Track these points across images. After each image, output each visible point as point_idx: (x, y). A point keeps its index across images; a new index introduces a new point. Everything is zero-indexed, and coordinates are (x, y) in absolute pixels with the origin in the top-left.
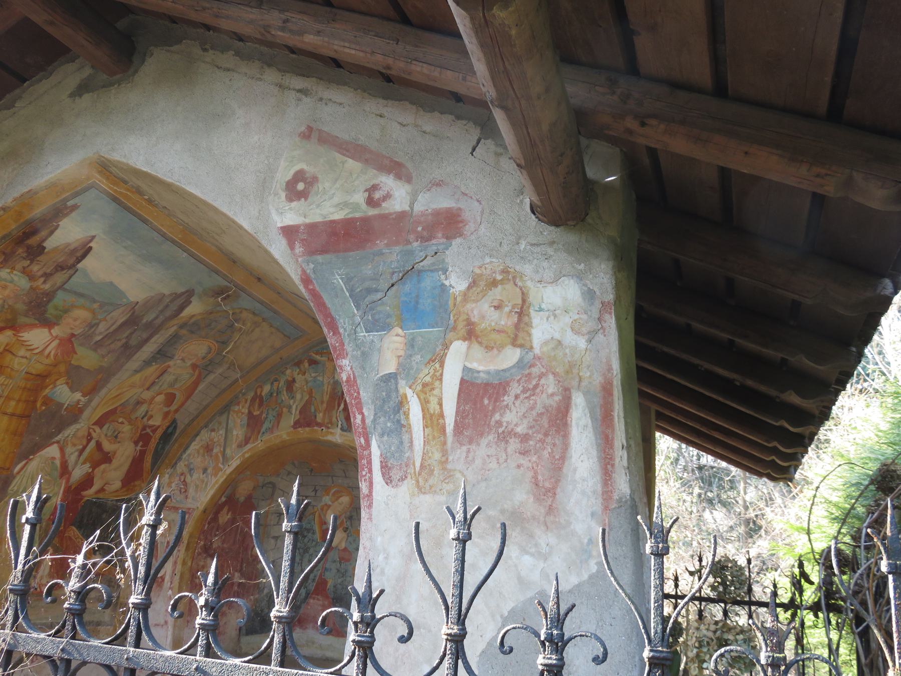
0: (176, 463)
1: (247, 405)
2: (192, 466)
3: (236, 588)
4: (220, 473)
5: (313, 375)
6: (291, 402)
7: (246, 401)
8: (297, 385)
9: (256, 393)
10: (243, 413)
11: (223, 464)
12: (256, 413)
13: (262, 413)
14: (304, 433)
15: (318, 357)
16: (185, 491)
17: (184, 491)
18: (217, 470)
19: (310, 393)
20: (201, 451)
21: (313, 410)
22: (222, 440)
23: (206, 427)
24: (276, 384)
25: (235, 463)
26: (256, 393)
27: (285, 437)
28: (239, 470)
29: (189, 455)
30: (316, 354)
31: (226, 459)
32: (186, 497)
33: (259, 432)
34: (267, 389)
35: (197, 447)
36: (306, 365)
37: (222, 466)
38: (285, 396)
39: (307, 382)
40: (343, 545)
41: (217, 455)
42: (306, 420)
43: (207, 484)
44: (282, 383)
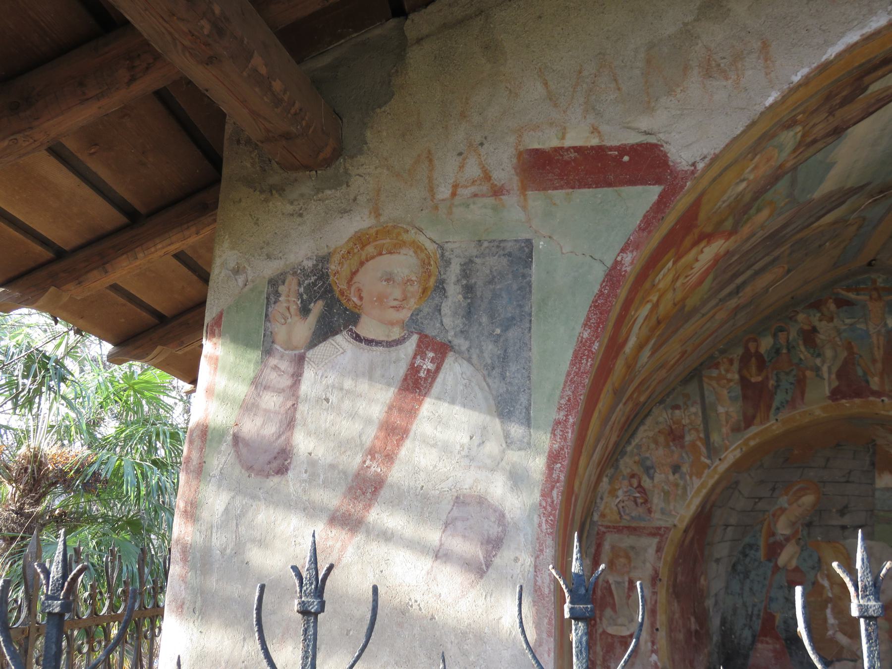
0: (617, 460)
1: (736, 366)
2: (648, 463)
3: (694, 640)
4: (706, 471)
5: (847, 321)
6: (818, 361)
7: (731, 362)
8: (822, 337)
9: (747, 349)
10: (729, 381)
11: (709, 457)
12: (756, 379)
13: (767, 378)
14: (851, 406)
15: (852, 296)
16: (646, 501)
17: (643, 498)
18: (698, 469)
19: (849, 347)
20: (661, 439)
21: (860, 373)
22: (699, 421)
23: (661, 402)
24: (782, 336)
25: (731, 456)
26: (747, 349)
27: (818, 413)
28: (737, 466)
29: (639, 446)
30: (849, 289)
31: (713, 451)
32: (650, 511)
33: (769, 407)
34: (766, 344)
35: (651, 434)
36: (832, 306)
37: (708, 461)
38: (803, 352)
39: (839, 332)
40: (794, 563)
41: (693, 445)
42: (849, 385)
43: (685, 489)
44: (793, 334)
